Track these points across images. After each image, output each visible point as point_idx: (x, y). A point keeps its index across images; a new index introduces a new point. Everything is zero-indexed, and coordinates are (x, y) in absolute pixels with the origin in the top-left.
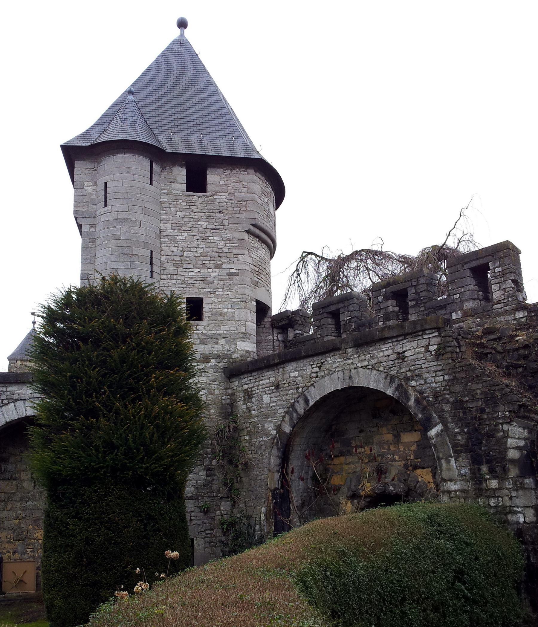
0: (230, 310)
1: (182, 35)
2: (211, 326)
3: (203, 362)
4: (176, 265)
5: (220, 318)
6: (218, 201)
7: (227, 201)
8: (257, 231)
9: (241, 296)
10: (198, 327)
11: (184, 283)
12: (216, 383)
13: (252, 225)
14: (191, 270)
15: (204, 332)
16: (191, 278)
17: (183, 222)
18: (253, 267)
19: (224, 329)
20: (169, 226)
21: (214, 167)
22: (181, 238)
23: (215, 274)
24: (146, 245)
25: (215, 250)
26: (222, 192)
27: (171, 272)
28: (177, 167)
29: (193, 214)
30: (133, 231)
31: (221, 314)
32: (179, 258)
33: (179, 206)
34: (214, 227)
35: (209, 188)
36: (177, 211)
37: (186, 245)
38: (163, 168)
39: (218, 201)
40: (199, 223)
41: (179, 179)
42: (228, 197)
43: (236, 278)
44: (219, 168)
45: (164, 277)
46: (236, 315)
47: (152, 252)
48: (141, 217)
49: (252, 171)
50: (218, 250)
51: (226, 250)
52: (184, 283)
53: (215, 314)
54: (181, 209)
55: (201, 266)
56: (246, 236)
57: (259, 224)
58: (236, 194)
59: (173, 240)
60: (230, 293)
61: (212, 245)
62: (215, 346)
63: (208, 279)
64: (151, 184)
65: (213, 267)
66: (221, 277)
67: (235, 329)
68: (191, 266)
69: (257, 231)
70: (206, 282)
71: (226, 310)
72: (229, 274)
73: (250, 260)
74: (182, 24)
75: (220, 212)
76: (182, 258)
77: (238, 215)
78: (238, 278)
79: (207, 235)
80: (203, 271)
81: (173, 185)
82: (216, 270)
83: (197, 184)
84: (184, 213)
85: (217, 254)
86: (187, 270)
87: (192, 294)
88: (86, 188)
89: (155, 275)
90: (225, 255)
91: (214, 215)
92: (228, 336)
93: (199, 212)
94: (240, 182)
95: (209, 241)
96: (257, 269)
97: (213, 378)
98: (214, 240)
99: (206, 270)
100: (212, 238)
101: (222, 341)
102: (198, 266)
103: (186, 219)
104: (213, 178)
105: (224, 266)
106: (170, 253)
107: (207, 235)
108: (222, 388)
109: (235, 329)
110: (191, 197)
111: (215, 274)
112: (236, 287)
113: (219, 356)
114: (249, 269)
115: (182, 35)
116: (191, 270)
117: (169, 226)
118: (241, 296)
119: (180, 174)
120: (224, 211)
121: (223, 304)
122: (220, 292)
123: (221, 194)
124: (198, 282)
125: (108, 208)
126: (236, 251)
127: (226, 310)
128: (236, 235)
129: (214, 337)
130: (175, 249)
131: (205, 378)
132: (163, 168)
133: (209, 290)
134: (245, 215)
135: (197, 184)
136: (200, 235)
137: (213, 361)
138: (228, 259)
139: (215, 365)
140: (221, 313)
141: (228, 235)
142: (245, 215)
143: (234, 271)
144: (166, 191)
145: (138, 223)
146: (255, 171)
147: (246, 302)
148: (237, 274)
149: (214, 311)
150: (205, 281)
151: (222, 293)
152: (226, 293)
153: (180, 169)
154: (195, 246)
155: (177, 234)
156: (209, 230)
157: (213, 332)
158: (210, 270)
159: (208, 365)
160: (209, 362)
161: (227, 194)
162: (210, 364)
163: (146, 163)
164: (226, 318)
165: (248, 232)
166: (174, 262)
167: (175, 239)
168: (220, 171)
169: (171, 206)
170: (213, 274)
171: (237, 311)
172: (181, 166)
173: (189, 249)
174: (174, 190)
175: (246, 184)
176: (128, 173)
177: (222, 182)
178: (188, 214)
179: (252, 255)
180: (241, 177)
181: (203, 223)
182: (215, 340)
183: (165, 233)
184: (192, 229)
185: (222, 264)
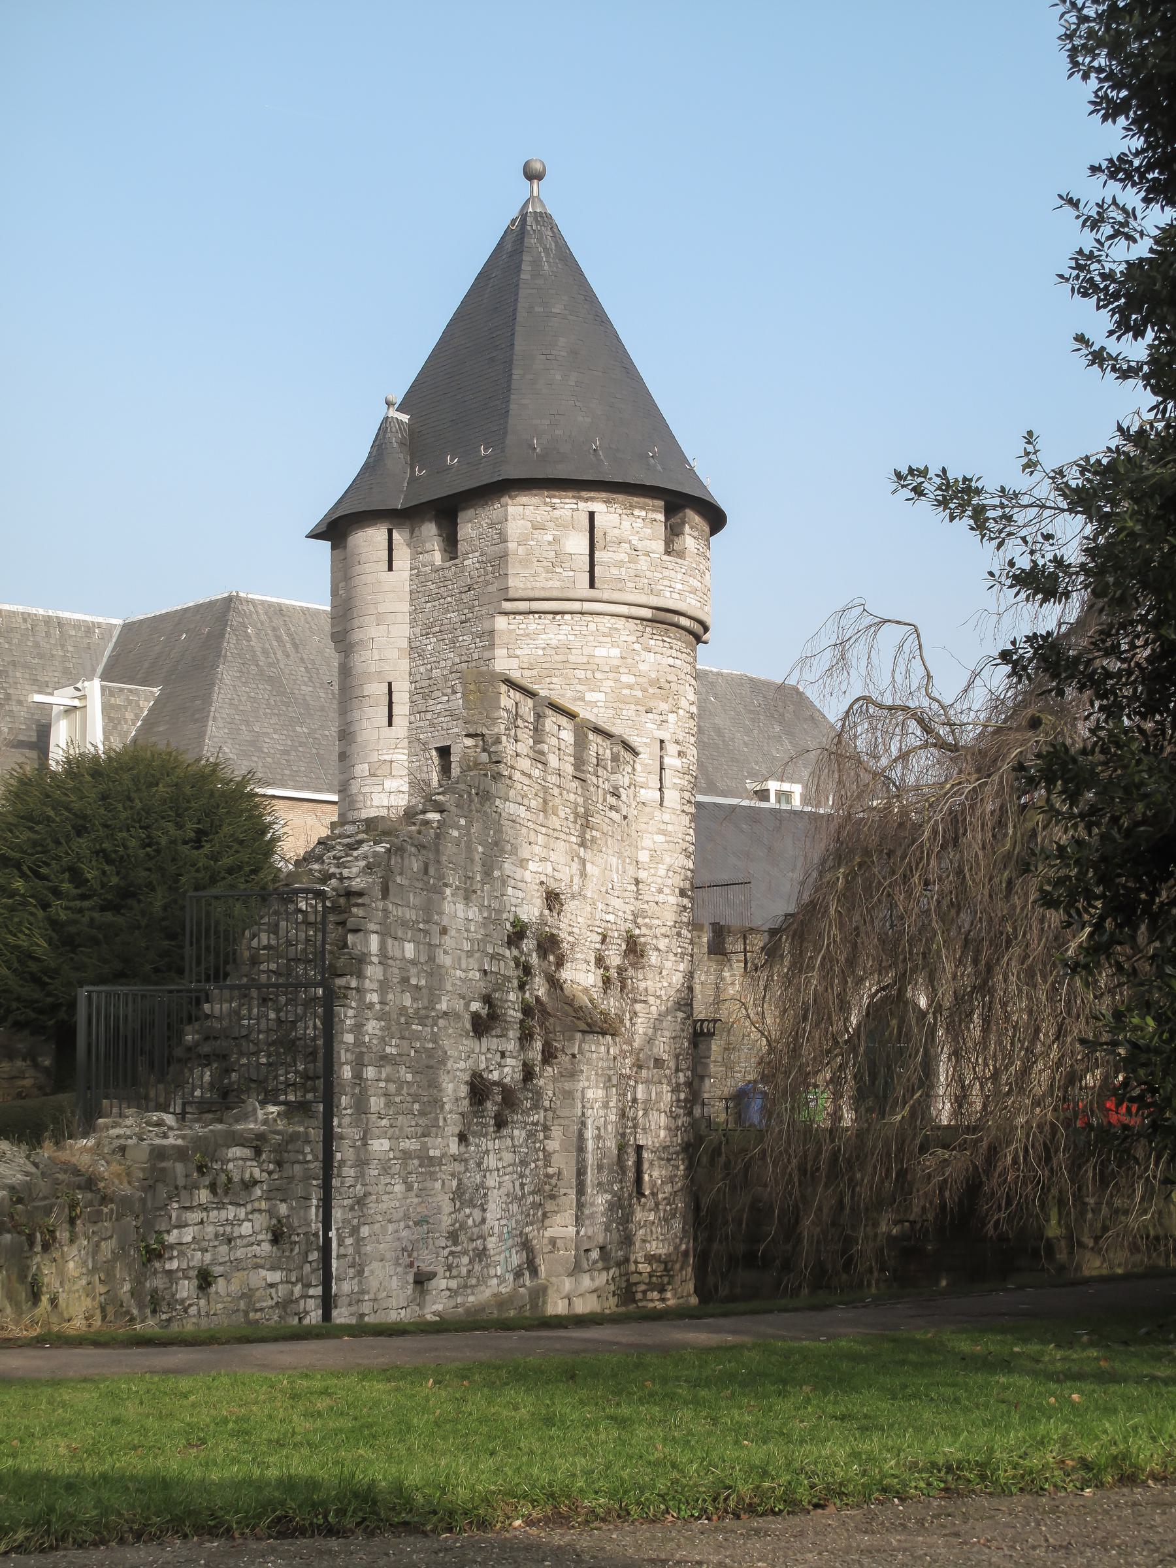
7: (477, 565)
21: (465, 509)
35: (462, 547)
45: (412, 717)
47: (390, 684)
56: (501, 622)
64: (390, 569)
74: (532, 175)
83: (451, 544)
89: (394, 718)
126: (487, 655)
128: (487, 625)
135: (451, 544)
155: (425, 642)
161: (477, 554)
168: (470, 513)
172: (430, 521)
178: (437, 603)
179: (518, 652)
181: (452, 615)
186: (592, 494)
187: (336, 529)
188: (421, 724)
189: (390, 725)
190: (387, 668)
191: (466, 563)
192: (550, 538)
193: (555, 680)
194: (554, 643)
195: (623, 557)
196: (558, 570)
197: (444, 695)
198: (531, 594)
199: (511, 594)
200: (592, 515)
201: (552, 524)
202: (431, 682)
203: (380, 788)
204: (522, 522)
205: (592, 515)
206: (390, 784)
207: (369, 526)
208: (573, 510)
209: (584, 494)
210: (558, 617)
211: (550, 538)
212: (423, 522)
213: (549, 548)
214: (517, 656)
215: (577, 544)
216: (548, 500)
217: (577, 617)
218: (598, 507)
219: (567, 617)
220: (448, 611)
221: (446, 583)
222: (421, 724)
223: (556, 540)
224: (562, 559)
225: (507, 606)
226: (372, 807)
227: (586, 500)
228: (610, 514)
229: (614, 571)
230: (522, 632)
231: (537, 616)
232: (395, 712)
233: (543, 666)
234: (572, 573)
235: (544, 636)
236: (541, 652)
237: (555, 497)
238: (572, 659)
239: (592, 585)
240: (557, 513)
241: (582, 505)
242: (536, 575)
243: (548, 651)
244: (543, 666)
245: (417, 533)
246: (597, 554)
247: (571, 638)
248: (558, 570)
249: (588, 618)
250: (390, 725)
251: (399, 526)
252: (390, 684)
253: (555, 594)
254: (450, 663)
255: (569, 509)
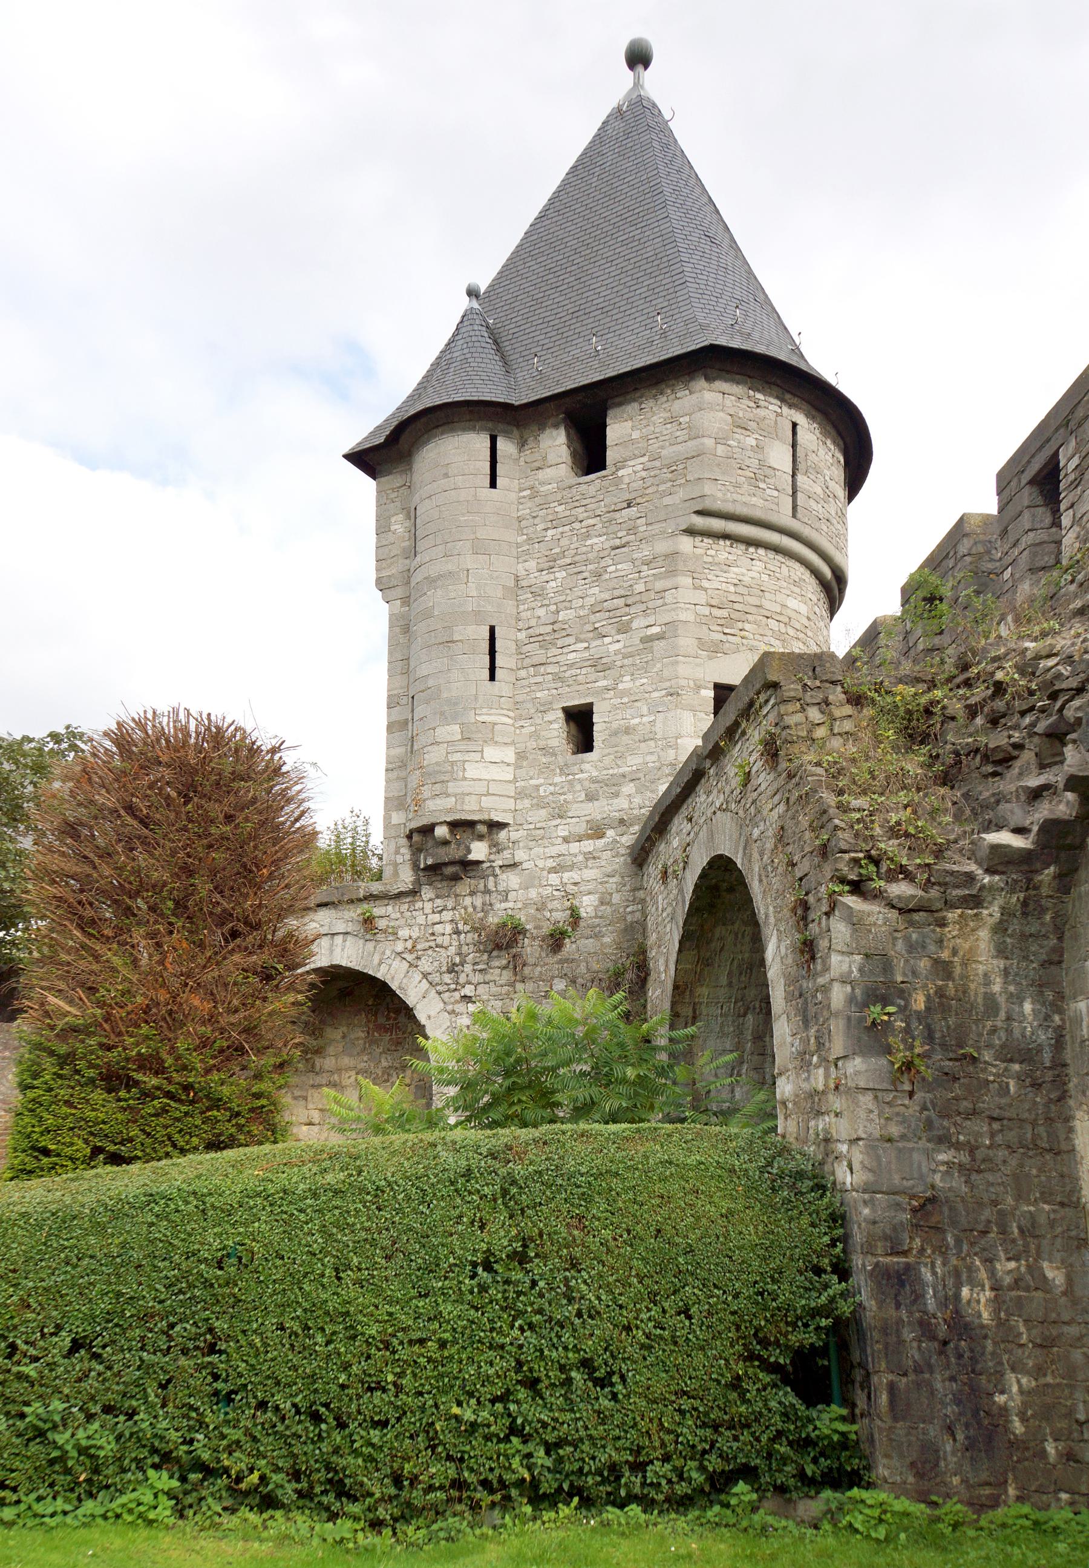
0: (645, 719)
1: (637, 84)
2: (607, 761)
3: (589, 837)
4: (544, 644)
5: (626, 739)
6: (626, 480)
7: (644, 474)
8: (717, 524)
9: (668, 684)
10: (583, 767)
11: (558, 678)
12: (614, 880)
13: (699, 513)
14: (572, 648)
15: (594, 774)
16: (571, 666)
17: (557, 550)
18: (706, 611)
19: (633, 762)
20: (532, 565)
21: (620, 404)
22: (553, 584)
23: (617, 646)
24: (478, 616)
25: (617, 593)
26: (636, 457)
27: (536, 660)
28: (548, 431)
29: (577, 525)
30: (452, 595)
31: (628, 731)
32: (549, 628)
33: (551, 517)
34: (618, 542)
35: (611, 455)
36: (546, 530)
37: (562, 598)
38: (522, 444)
39: (626, 480)
40: (589, 542)
41: (552, 458)
42: (649, 465)
43: (659, 645)
44: (629, 402)
45: (523, 673)
46: (659, 727)
47: (492, 630)
48: (469, 561)
49: (702, 383)
50: (623, 593)
51: (640, 587)
52: (558, 678)
53: (615, 733)
54: (555, 522)
55: (591, 635)
56: (686, 544)
57: (718, 506)
58: (664, 452)
59: (538, 594)
60: (645, 681)
61: (612, 584)
62: (616, 801)
63: (604, 661)
64: (493, 484)
65: (613, 632)
66: (630, 650)
67: (654, 758)
68: (571, 640)
69: (717, 524)
70: (599, 668)
71: (637, 721)
72: (647, 640)
73: (701, 597)
75: (629, 506)
76: (556, 627)
77: (667, 500)
78: (662, 643)
79: (603, 564)
80: (594, 644)
81: (541, 475)
82: (619, 637)
84: (560, 530)
85: (621, 602)
86: (565, 650)
87: (573, 698)
88: (393, 528)
89: (499, 673)
90: (638, 598)
91: (617, 515)
92: (641, 775)
93: (589, 518)
94: (673, 420)
95: (607, 576)
96: (724, 613)
97: (609, 869)
98: (617, 570)
99: (599, 642)
100: (612, 568)
101: (628, 788)
102: (582, 636)
103: (564, 542)
104: (620, 430)
105: (635, 625)
106: (533, 622)
107: (603, 564)
108: (628, 888)
109: (654, 758)
110: (574, 490)
111: (617, 646)
112: (659, 665)
113: (622, 821)
114: (691, 617)
115: (637, 84)
116: (572, 648)
117: (532, 565)
118: (668, 684)
119: (556, 443)
120: (638, 500)
121: (631, 707)
122: (626, 684)
123: (631, 463)
124: (584, 671)
125: (418, 558)
126: (659, 585)
127: (637, 721)
128: (662, 547)
129: (614, 781)
130: (541, 612)
131: (595, 871)
132: (522, 444)
133: (603, 683)
134: (681, 494)
136: (590, 567)
137: (610, 833)
138: (643, 607)
139: (615, 841)
140: (627, 728)
141: (646, 552)
142: (681, 494)
143: (655, 630)
144: (528, 492)
145: (463, 575)
146: (709, 379)
147: (678, 694)
148: (660, 637)
149: (615, 725)
150: (599, 665)
151: (630, 685)
152: (638, 683)
153: (555, 432)
154: (580, 594)
155: (546, 578)
156: (606, 553)
157: (611, 772)
158: (607, 640)
159: (600, 843)
160: (601, 836)
161: (646, 459)
162: (603, 841)
163: (476, 443)
164: (637, 738)
165: (691, 532)
166: (540, 638)
167: (543, 589)
168: (632, 408)
169: (536, 521)
170: (613, 646)
171: (660, 716)
172: (556, 426)
173: (567, 604)
174: (542, 484)
175: (687, 419)
176: (446, 476)
177: (636, 435)
178: (567, 528)
179: (705, 584)
180: (677, 406)
181: (595, 540)
182: (613, 789)
183: (524, 583)
184: (577, 558)
185: (631, 621)
186: (796, 400)
187: (384, 456)
188: (539, 679)
189: (492, 678)
190: (489, 608)
191: (620, 473)
192: (754, 443)
193: (747, 626)
194: (747, 580)
195: (819, 491)
196: (762, 485)
197: (579, 640)
198: (729, 508)
199: (708, 504)
200: (795, 425)
201: (753, 425)
202: (556, 627)
203: (477, 756)
204: (721, 414)
205: (795, 425)
206: (491, 753)
207: (464, 430)
208: (779, 415)
209: (788, 396)
210: (752, 549)
211: (754, 443)
212: (542, 428)
213: (751, 454)
214: (706, 590)
215: (780, 457)
216: (751, 393)
217: (771, 554)
218: (800, 418)
219: (761, 551)
220: (588, 536)
221: (585, 502)
222: (539, 679)
223: (759, 447)
224: (762, 474)
225: (700, 522)
226: (465, 779)
227: (790, 406)
228: (810, 434)
229: (812, 503)
230: (710, 559)
231: (728, 543)
232: (499, 662)
233: (737, 606)
234: (776, 493)
235: (735, 569)
236: (732, 589)
237: (759, 391)
238: (767, 604)
239: (794, 516)
240: (761, 412)
241: (786, 410)
242: (738, 486)
243: (740, 589)
244: (737, 606)
245: (531, 443)
246: (800, 478)
247: (765, 577)
248: (762, 485)
249: (779, 557)
250: (492, 678)
251: (507, 434)
252: (492, 630)
253: (758, 514)
254: (592, 600)
255: (773, 411)
